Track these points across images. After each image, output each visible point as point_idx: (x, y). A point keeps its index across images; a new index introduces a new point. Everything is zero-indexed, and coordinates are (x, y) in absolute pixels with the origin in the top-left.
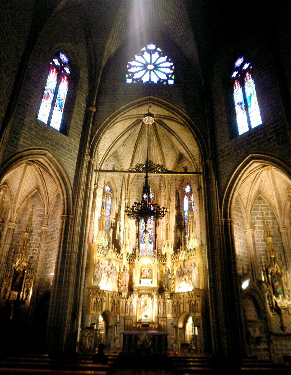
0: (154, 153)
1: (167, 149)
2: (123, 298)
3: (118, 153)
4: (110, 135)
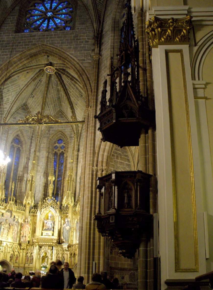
0: (64, 103)
1: (76, 98)
2: (23, 249)
3: (28, 105)
4: (13, 88)
